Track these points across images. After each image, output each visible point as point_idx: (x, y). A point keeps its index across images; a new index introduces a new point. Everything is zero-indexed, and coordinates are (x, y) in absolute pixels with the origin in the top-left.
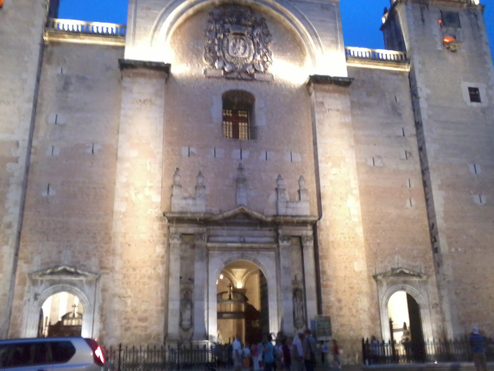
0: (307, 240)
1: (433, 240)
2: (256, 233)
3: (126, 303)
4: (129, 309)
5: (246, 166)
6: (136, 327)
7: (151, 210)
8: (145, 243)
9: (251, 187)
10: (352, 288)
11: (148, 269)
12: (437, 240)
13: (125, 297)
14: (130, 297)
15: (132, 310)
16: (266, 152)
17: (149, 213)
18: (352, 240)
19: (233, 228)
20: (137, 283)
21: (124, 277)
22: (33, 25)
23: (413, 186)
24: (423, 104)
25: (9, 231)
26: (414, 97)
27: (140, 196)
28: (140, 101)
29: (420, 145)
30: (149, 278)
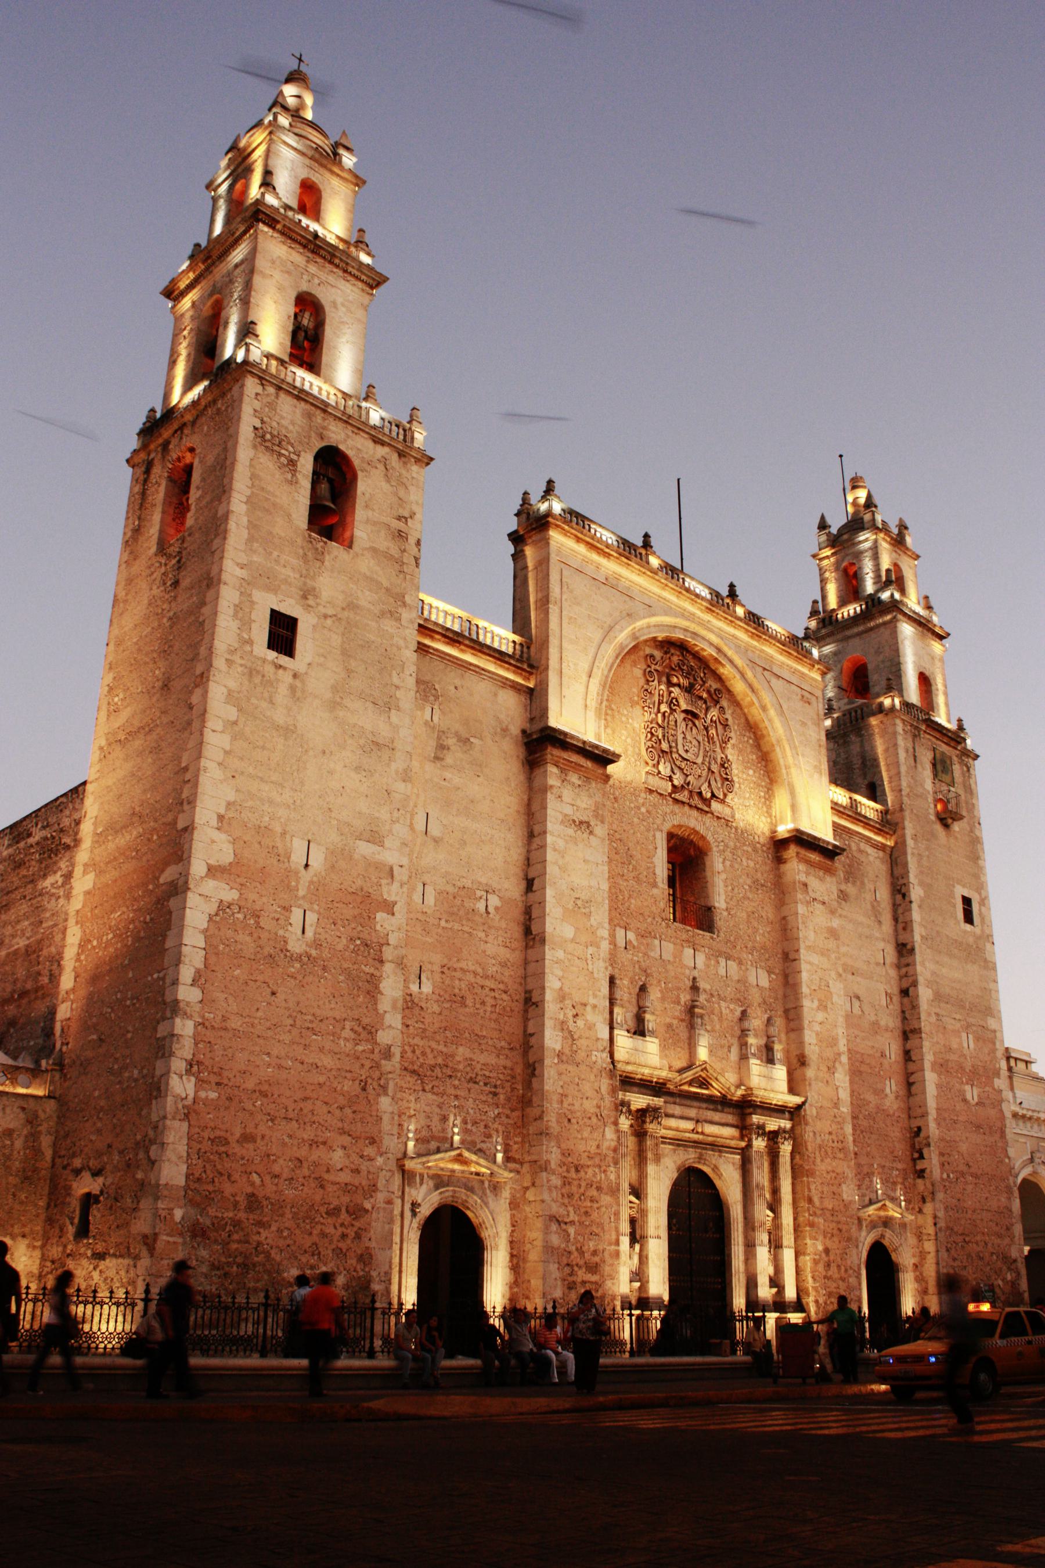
0: (785, 1139)
1: (916, 1155)
2: (717, 1116)
3: (569, 1235)
4: (574, 1248)
5: (702, 985)
9: (709, 1028)
11: (597, 1170)
12: (926, 1155)
13: (566, 1223)
14: (572, 1223)
15: (577, 1249)
17: (594, 1058)
18: (840, 1145)
19: (688, 1102)
22: (404, 604)
23: (893, 1057)
24: (916, 915)
25: (386, 1065)
26: (899, 897)
27: (580, 1023)
28: (574, 821)
29: (905, 985)
30: (599, 1189)
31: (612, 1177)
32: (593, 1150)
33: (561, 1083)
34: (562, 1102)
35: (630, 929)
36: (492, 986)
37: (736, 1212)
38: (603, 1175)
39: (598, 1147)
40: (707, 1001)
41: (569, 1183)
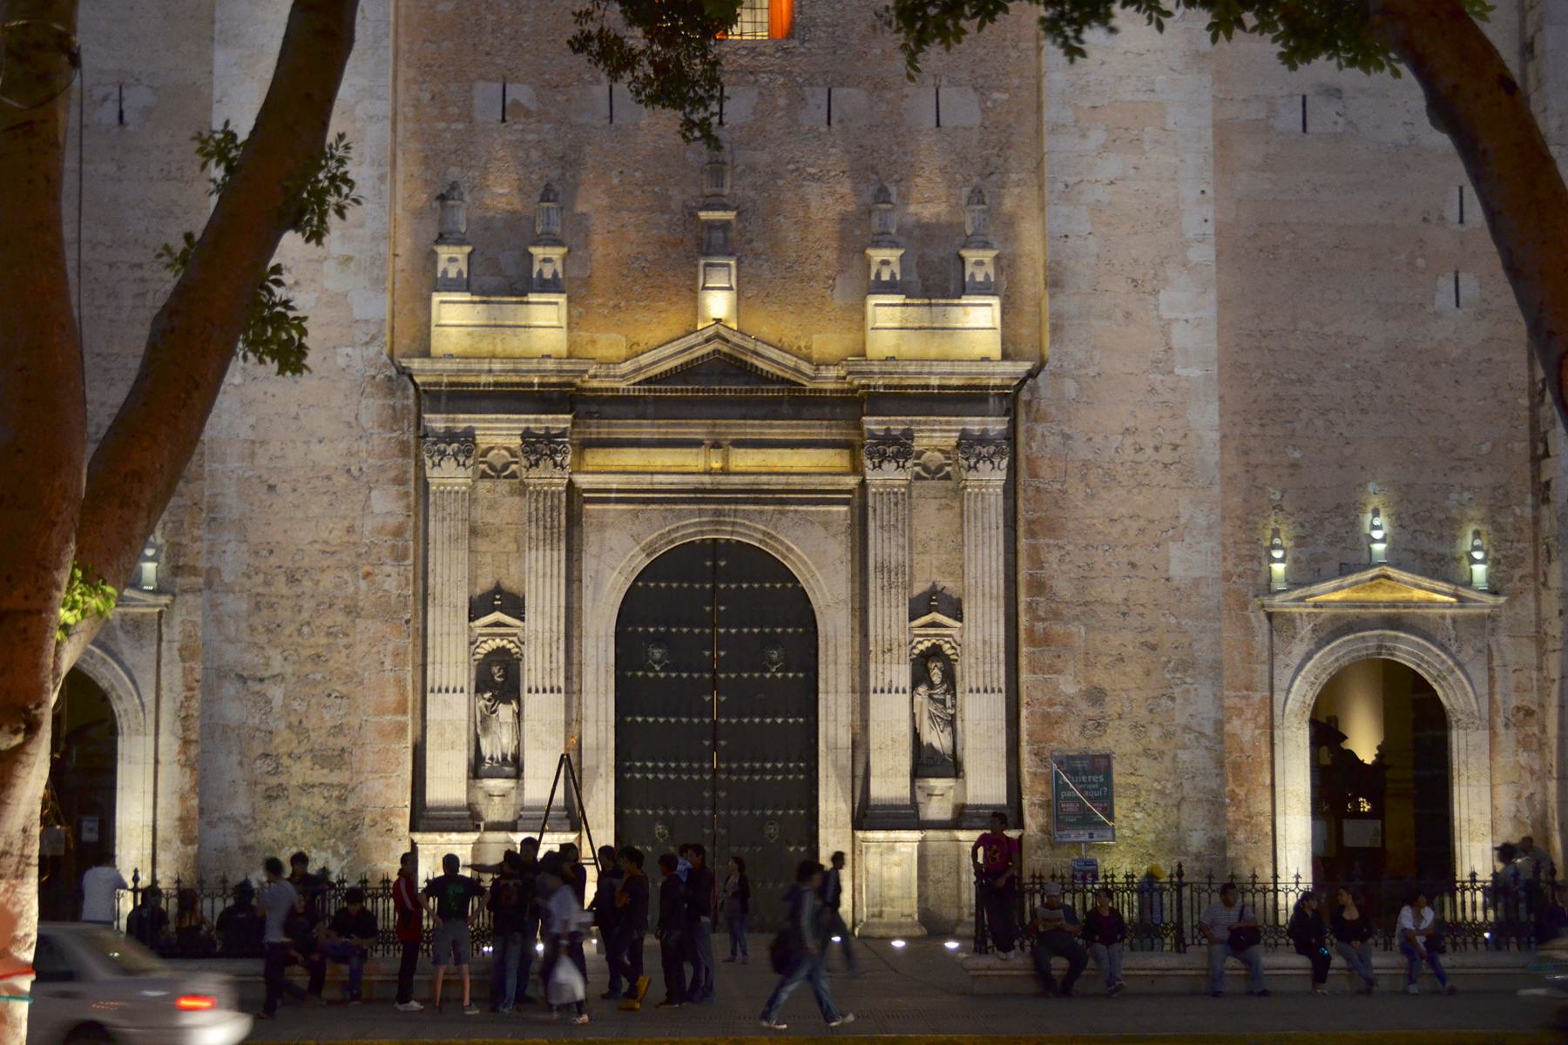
3: (268, 702)
6: (306, 788)
7: (349, 350)
8: (329, 478)
10: (1153, 647)
11: (346, 575)
13: (261, 680)
14: (278, 678)
16: (829, 91)
17: (341, 361)
18: (1167, 455)
20: (306, 630)
21: (258, 607)
30: (352, 611)
31: (391, 585)
32: (338, 536)
33: (252, 420)
34: (253, 455)
35: (516, 80)
36: (135, 260)
37: (834, 624)
38: (363, 584)
39: (350, 530)
40: (754, 187)
41: (271, 606)
